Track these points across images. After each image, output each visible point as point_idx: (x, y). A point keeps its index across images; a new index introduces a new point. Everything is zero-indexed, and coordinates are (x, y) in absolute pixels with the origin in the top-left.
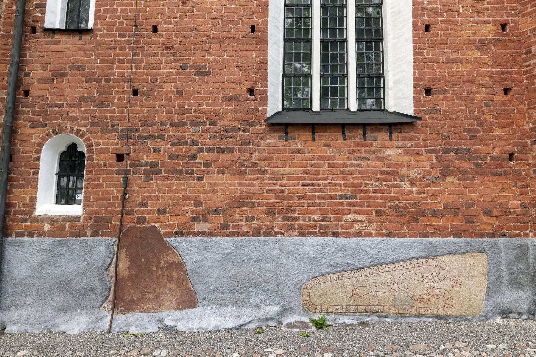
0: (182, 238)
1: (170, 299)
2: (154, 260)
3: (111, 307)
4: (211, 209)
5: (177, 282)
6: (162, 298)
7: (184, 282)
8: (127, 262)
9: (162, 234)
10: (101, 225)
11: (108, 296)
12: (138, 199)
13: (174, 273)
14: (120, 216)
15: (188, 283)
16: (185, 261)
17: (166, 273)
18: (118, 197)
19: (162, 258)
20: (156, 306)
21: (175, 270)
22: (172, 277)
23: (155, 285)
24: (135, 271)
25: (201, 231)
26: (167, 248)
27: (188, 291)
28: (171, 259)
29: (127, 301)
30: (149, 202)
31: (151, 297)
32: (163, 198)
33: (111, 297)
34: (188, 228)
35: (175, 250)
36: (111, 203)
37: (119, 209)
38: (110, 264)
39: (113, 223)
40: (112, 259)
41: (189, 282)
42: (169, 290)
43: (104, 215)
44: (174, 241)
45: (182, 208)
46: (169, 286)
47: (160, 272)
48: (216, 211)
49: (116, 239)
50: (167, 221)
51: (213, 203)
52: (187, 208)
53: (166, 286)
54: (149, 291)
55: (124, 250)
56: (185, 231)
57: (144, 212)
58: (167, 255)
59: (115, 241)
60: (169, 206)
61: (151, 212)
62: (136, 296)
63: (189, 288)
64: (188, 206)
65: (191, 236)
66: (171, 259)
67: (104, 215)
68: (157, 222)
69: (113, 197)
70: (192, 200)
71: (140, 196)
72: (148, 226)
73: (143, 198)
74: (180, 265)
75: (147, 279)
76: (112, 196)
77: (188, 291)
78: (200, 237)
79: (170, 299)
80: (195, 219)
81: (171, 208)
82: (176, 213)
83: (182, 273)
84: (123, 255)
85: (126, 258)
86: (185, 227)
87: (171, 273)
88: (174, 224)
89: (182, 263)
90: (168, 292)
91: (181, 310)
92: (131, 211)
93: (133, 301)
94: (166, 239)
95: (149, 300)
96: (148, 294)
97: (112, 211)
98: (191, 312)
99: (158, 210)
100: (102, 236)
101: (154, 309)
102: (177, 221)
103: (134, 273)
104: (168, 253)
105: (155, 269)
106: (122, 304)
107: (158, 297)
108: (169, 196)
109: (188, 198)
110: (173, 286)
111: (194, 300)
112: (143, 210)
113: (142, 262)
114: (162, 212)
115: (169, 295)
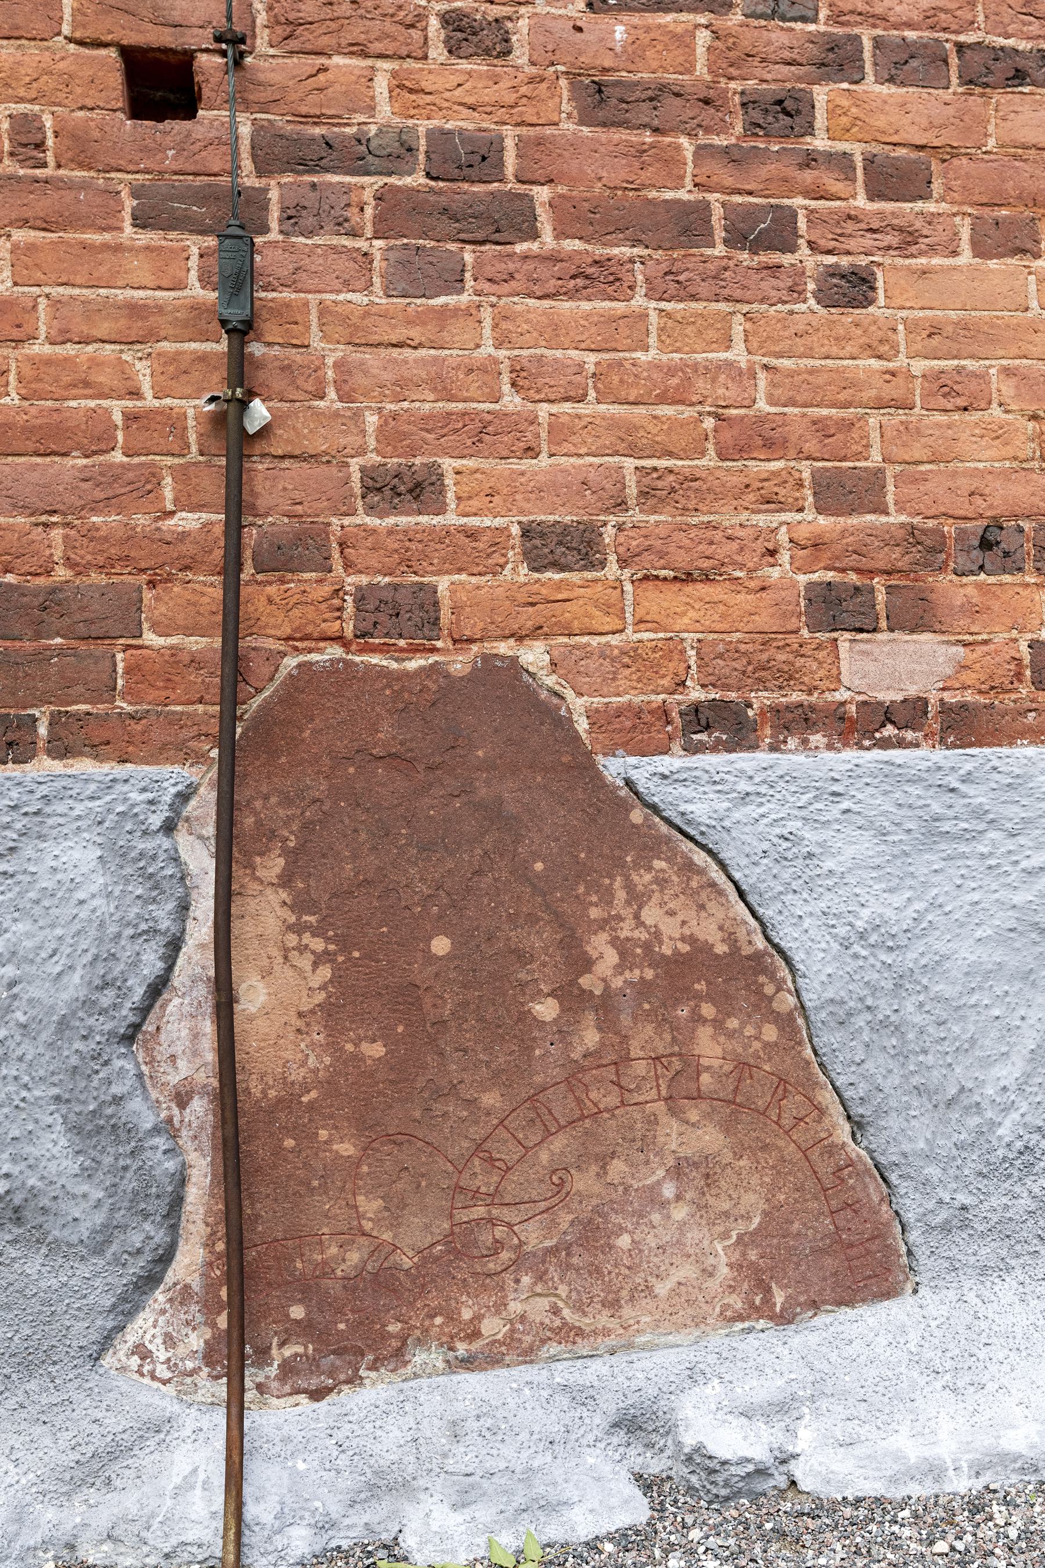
0: (744, 760)
1: (688, 1243)
2: (539, 940)
3: (196, 1341)
4: (949, 529)
5: (733, 1108)
6: (624, 1241)
7: (794, 1105)
8: (305, 962)
9: (582, 725)
10: (41, 657)
11: (166, 1258)
12: (353, 440)
13: (705, 1033)
14: (209, 588)
15: (822, 1112)
16: (787, 936)
17: (644, 1038)
18: (175, 423)
19: (603, 924)
20: (579, 1308)
21: (708, 1010)
22: (692, 1067)
23: (558, 1143)
24: (385, 1035)
25: (887, 696)
26: (631, 836)
27: (825, 1168)
28: (669, 922)
29: (333, 1287)
30: (448, 464)
31: (534, 1237)
32: (559, 432)
33: (190, 1263)
34: (788, 677)
35: (700, 858)
36: (115, 474)
37: (188, 521)
38: (158, 988)
39: (150, 638)
40: (175, 945)
41: (827, 1097)
42: (677, 1171)
43: (62, 573)
44: (693, 784)
45: (728, 519)
46: (675, 1137)
47: (591, 1038)
48: (986, 544)
49: (203, 777)
50: (611, 622)
51: (965, 485)
52: (762, 520)
53: (646, 1144)
54: (511, 1190)
55: (273, 866)
56: (761, 699)
57: (410, 553)
58: (637, 898)
59: (184, 797)
60: (621, 505)
61: (472, 550)
62: (413, 1238)
63: (832, 1149)
64: (770, 502)
65: (817, 739)
66: (670, 928)
67: (62, 573)
68: (536, 632)
69: (131, 418)
70: (802, 455)
71: (372, 420)
72: (459, 664)
73: (391, 435)
74: (748, 973)
75: (490, 1099)
76: (117, 409)
77: (825, 1168)
78: (885, 744)
79: (688, 1243)
80: (838, 610)
81: (635, 515)
82: (682, 560)
83: (770, 1033)
84: (265, 912)
85: (298, 929)
86: (762, 674)
87: (682, 1035)
88: (673, 649)
89: (758, 957)
90: (668, 1191)
91: (784, 1319)
92: (299, 539)
93: (382, 1282)
94: (614, 767)
95: (517, 1264)
97: (130, 537)
98: (866, 1330)
99: (527, 533)
100: (61, 750)
101: (568, 1333)
102: (690, 616)
103: (376, 1050)
104: (643, 879)
105: (546, 1010)
106: (297, 1312)
107: (593, 1234)
108: (613, 423)
109: (769, 440)
110: (709, 1138)
111: (880, 1234)
112: (408, 535)
113: (430, 958)
115: (680, 1213)
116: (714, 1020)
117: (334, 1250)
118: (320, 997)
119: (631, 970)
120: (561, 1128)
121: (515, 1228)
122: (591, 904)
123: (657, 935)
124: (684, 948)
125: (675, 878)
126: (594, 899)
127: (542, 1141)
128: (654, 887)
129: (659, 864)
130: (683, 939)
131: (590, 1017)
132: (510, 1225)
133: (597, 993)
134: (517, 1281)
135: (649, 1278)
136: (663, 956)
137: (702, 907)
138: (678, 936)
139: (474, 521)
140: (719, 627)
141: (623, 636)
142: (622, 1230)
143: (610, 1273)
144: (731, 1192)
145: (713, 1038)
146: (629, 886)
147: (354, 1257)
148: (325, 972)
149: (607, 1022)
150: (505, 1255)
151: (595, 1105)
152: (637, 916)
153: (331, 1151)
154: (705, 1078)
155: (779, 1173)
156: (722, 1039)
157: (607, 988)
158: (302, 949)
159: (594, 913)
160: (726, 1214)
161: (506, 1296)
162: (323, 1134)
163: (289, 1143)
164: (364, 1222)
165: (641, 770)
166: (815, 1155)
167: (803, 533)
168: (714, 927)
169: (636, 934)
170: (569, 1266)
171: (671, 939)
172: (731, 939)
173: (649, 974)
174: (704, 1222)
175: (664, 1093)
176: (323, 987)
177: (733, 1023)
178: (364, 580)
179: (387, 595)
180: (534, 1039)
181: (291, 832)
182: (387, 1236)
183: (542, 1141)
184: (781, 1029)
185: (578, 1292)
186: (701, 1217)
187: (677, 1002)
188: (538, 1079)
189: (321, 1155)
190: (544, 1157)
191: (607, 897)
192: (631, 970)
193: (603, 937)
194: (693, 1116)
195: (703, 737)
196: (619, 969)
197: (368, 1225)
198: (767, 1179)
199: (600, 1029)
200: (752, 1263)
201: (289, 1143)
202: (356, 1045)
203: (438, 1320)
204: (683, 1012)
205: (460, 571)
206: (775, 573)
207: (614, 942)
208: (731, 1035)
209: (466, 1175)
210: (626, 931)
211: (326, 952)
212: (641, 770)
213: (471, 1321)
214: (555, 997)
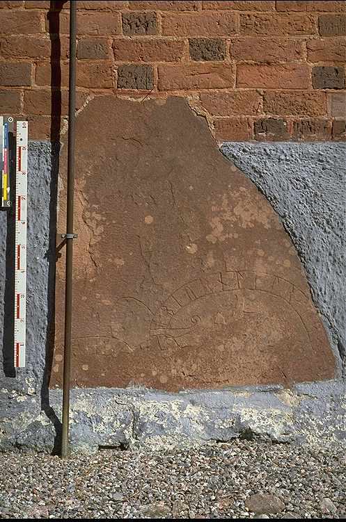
6: (221, 348)
8: (93, 224)
13: (259, 262)
19: (218, 213)
21: (261, 252)
23: (195, 305)
52: (294, 38)
58: (232, 204)
61: (168, 51)
66: (246, 216)
72: (162, 100)
83: (287, 263)
105: (192, 249)
114: (205, 50)
116: (263, 257)
122: (213, 205)
123: (240, 219)
124: (252, 225)
125: (249, 195)
126: (214, 203)
128: (240, 199)
129: (242, 189)
131: (211, 253)
133: (214, 243)
134: (176, 361)
137: (260, 208)
138: (249, 220)
139: (170, 38)
140: (273, 86)
141: (231, 90)
142: (220, 343)
145: (263, 265)
146: (229, 197)
147: (109, 347)
148: (101, 228)
151: (211, 290)
152: (232, 211)
153: (101, 303)
157: (218, 240)
158: (92, 219)
159: (214, 209)
163: (84, 298)
165: (235, 148)
167: (312, 45)
171: (246, 221)
172: (272, 222)
177: (271, 259)
178: (122, 63)
179: (132, 70)
181: (89, 170)
189: (97, 304)
191: (219, 204)
195: (264, 134)
196: (224, 232)
199: (214, 258)
201: (84, 298)
202: (113, 260)
203: (142, 375)
204: (250, 253)
205: (162, 60)
206: (299, 62)
207: (222, 221)
208: (270, 264)
210: (227, 216)
211: (102, 220)
212: (235, 148)
214: (196, 243)
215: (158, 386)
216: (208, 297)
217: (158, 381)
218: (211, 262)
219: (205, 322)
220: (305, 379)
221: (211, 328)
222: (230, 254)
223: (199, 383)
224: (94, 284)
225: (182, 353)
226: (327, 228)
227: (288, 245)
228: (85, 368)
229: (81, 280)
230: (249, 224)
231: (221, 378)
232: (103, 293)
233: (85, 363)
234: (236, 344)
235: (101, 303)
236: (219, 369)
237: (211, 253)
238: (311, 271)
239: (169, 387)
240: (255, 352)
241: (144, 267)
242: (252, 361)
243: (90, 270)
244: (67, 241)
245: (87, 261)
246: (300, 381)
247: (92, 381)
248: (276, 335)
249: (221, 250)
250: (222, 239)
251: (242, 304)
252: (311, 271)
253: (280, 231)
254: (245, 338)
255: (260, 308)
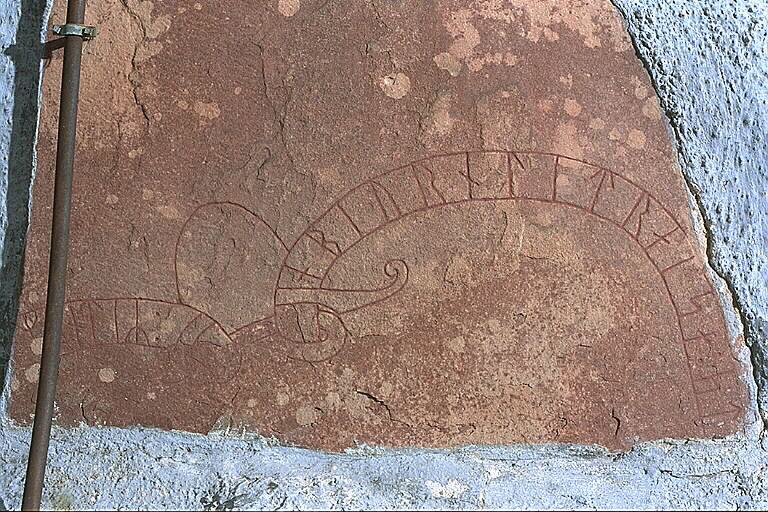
6: (458, 345)
7: (657, 221)
13: (566, 131)
15: (683, 229)
21: (572, 107)
23: (396, 232)
29: (147, 356)
54: (340, 273)
83: (638, 140)
96: (335, 301)
105: (395, 86)
117: (150, 316)
118: (157, 49)
119: (493, 54)
120: (402, 216)
121: (342, 316)
127: (379, 228)
130: (552, 28)
132: (336, 312)
134: (339, 373)
135: (480, 386)
136: (527, 42)
142: (455, 332)
143: (439, 375)
144: (576, 306)
145: (576, 137)
147: (169, 326)
149: (465, 108)
150: (328, 345)
154: (562, 180)
155: (632, 292)
156: (585, 140)
160: (570, 329)
161: (326, 387)
162: (148, 194)
164: (182, 291)
166: (673, 277)
168: (587, 17)
169: (501, 15)
170: (395, 363)
172: (604, 32)
173: (512, 61)
174: (545, 334)
175: (516, 193)
176: (161, 39)
177: (597, 124)
180: (381, 117)
182: (203, 307)
183: (379, 228)
184: (650, 137)
185: (403, 392)
186: (543, 328)
187: (541, 95)
188: (380, 160)
190: (380, 244)
192: (493, 54)
193: (464, 14)
194: (546, 218)
197: (187, 295)
198: (619, 298)
199: (453, 114)
200: (594, 384)
203: (252, 403)
204: (546, 105)
207: (476, 21)
208: (594, 137)
209: (297, 254)
213: (287, 407)
214: (407, 73)
215: (286, 431)
216: (429, 214)
217: (292, 423)
218: (443, 123)
219: (422, 278)
220: (665, 434)
221: (435, 293)
222: (492, 107)
223: (391, 425)
224: (139, 163)
225: (357, 353)
226: (741, 56)
227: (641, 92)
228: (107, 375)
229: (104, 152)
230: (547, 32)
231: (454, 419)
232: (161, 188)
233: (106, 364)
234: (496, 335)
235: (154, 213)
236: (450, 399)
237: (444, 101)
238: (696, 162)
239: (325, 435)
240: (543, 360)
241: (269, 128)
242: (533, 382)
243: (131, 128)
244: (65, 43)
245: (123, 101)
246: (651, 435)
247: (128, 408)
248: (600, 319)
249: (472, 95)
250: (477, 65)
251: (517, 236)
252: (696, 162)
253: (624, 55)
254: (519, 323)
255: (565, 250)
